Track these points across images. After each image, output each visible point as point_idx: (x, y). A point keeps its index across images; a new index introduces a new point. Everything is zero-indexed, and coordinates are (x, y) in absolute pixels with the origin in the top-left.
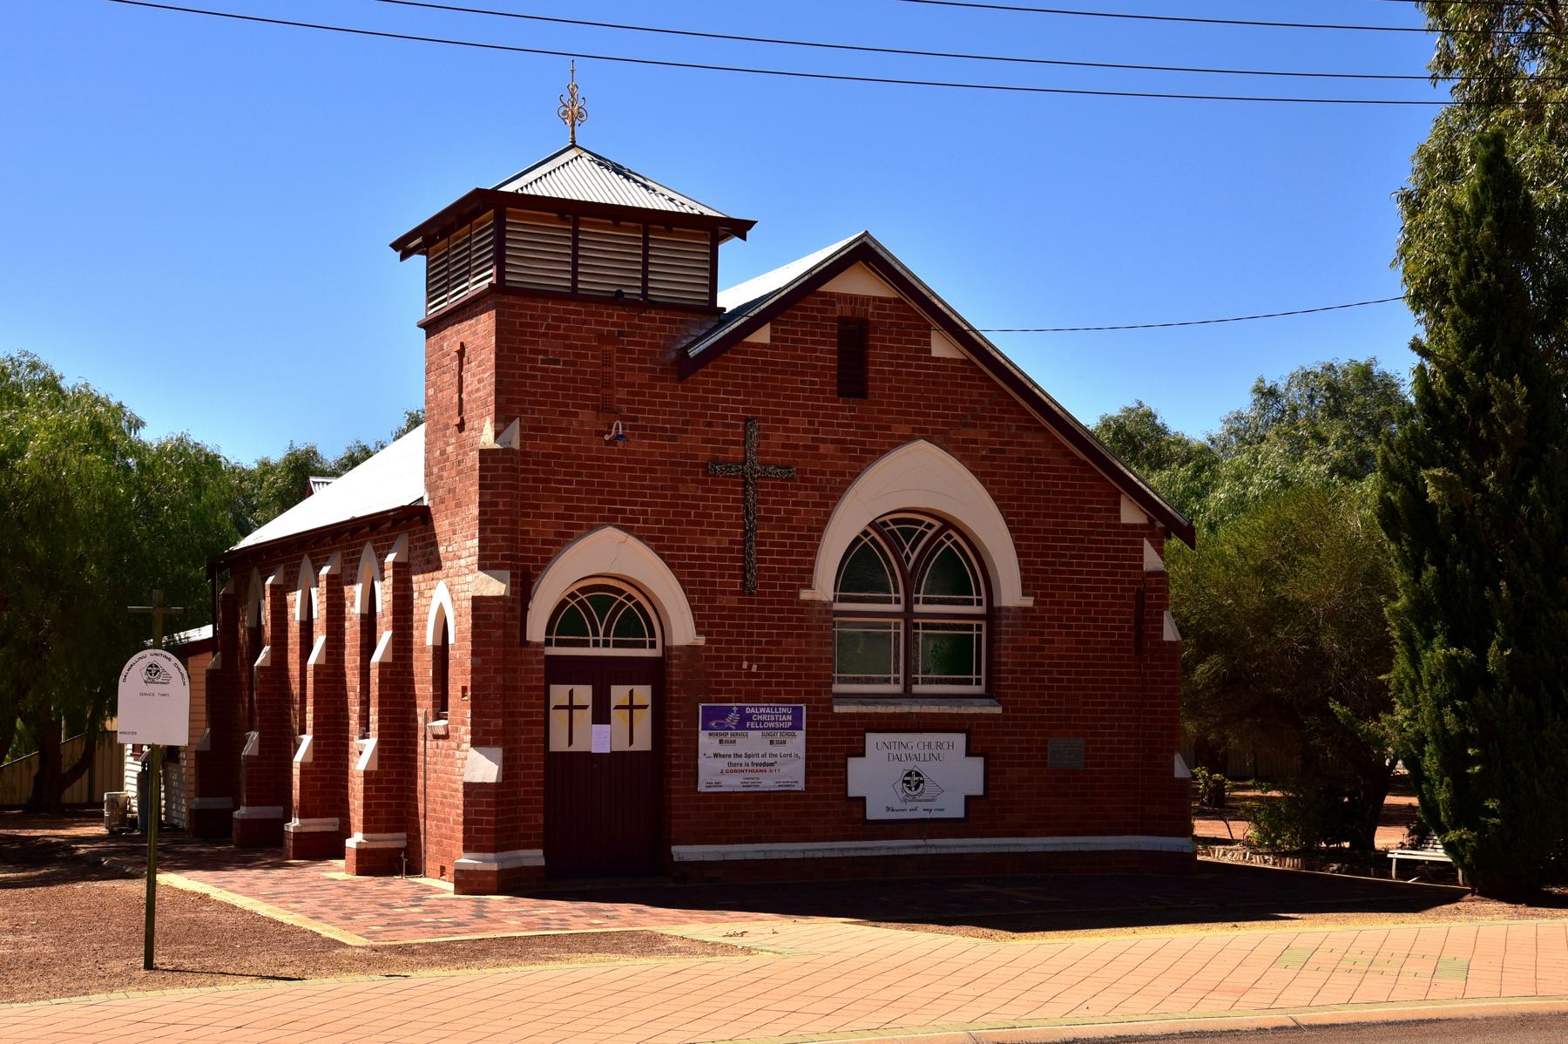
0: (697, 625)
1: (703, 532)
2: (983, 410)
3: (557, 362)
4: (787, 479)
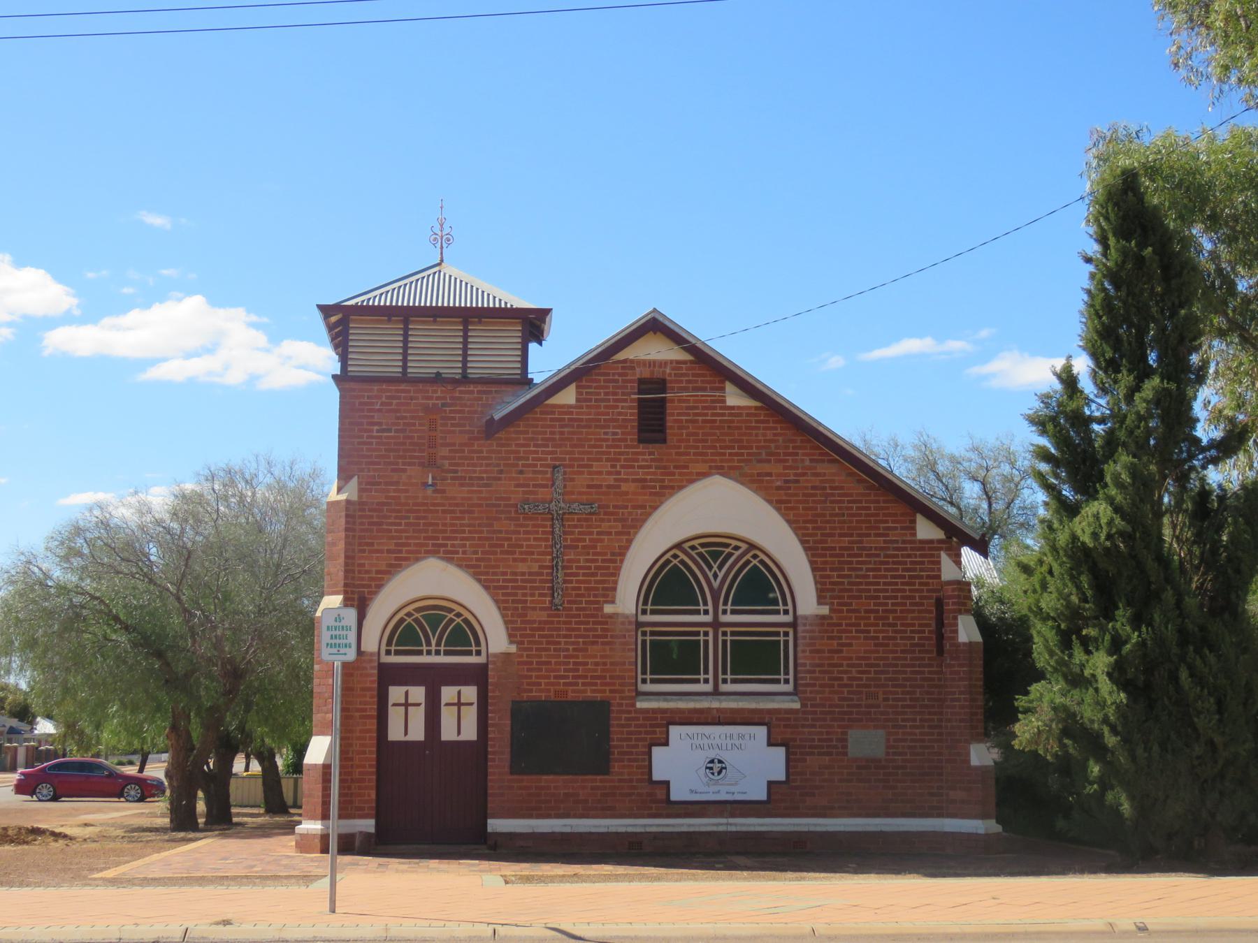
0: (510, 636)
1: (515, 560)
2: (777, 447)
3: (389, 430)
4: (591, 514)
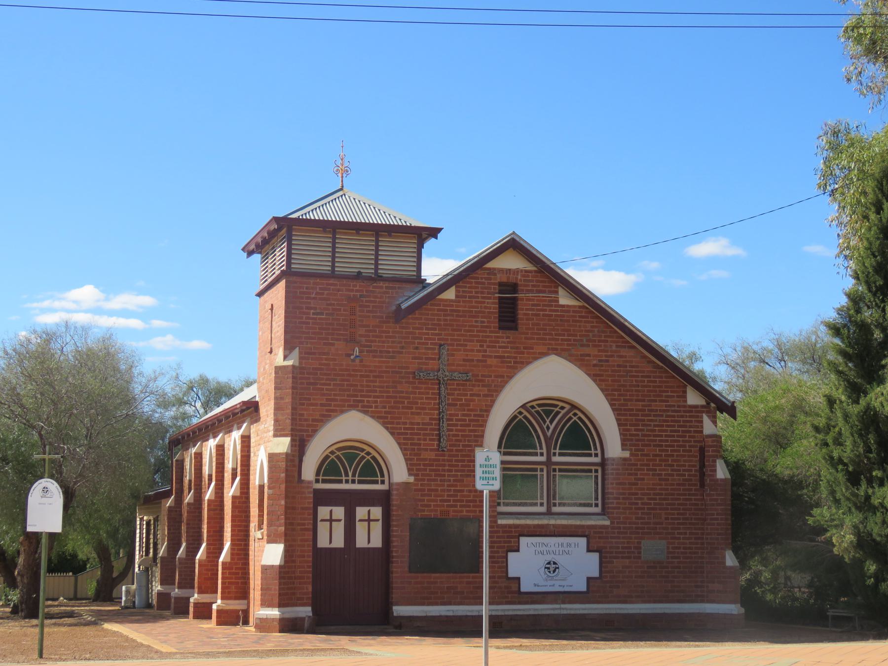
0: (409, 470)
2: (594, 336)
3: (322, 314)
4: (466, 380)
